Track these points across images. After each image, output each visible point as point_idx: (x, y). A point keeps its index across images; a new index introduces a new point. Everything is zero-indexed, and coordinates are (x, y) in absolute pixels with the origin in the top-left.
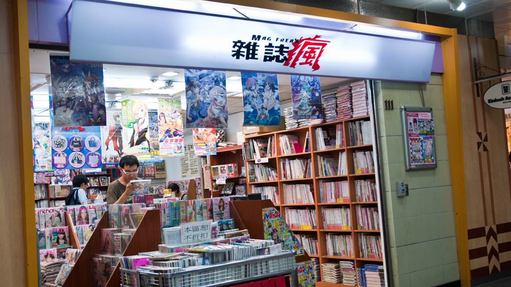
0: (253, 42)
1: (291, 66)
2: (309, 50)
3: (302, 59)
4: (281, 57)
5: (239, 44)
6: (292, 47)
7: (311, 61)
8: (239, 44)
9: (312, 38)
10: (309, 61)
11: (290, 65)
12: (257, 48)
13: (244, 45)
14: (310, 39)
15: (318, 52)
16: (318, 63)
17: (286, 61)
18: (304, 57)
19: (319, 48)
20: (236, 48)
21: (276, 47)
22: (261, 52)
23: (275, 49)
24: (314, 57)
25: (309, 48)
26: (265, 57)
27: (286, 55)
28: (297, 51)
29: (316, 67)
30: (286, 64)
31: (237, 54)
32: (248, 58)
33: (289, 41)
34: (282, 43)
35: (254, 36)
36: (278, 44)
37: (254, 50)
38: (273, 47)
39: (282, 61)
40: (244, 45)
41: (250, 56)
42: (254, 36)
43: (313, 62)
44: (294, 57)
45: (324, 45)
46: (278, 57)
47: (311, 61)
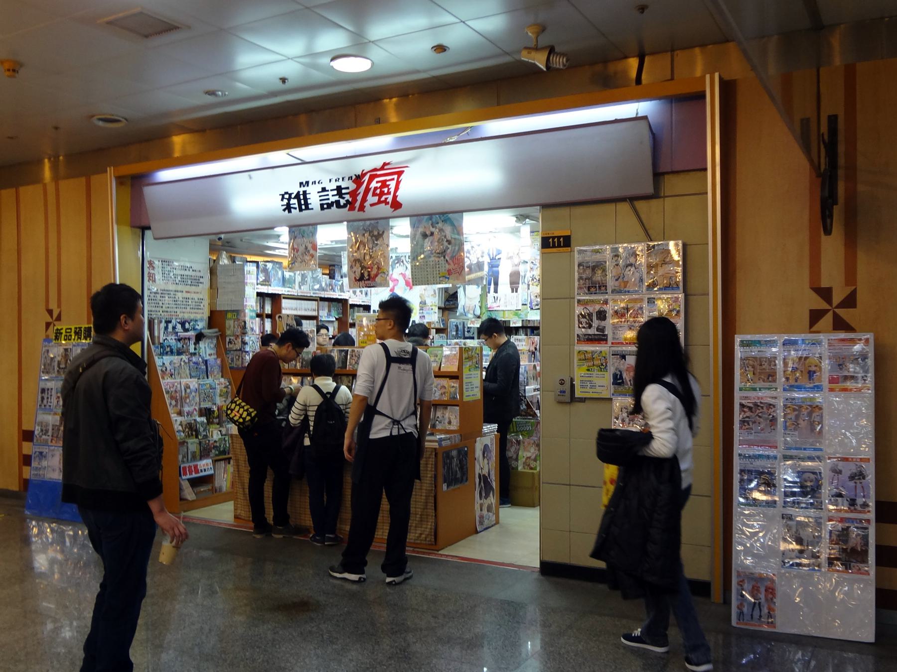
0: (302, 190)
1: (359, 210)
3: (371, 199)
4: (342, 202)
6: (353, 186)
7: (386, 199)
10: (383, 199)
13: (293, 196)
14: (375, 170)
15: (392, 185)
16: (398, 199)
17: (350, 205)
18: (374, 194)
19: (393, 179)
20: (285, 201)
22: (314, 200)
23: (331, 193)
24: (389, 193)
25: (377, 182)
26: (322, 205)
27: (347, 197)
30: (352, 208)
31: (288, 208)
32: (301, 210)
34: (338, 184)
35: (301, 184)
37: (306, 199)
39: (345, 206)
40: (293, 196)
41: (303, 207)
42: (301, 184)
43: (390, 198)
44: (359, 198)
45: (400, 174)
46: (337, 202)
47: (386, 199)
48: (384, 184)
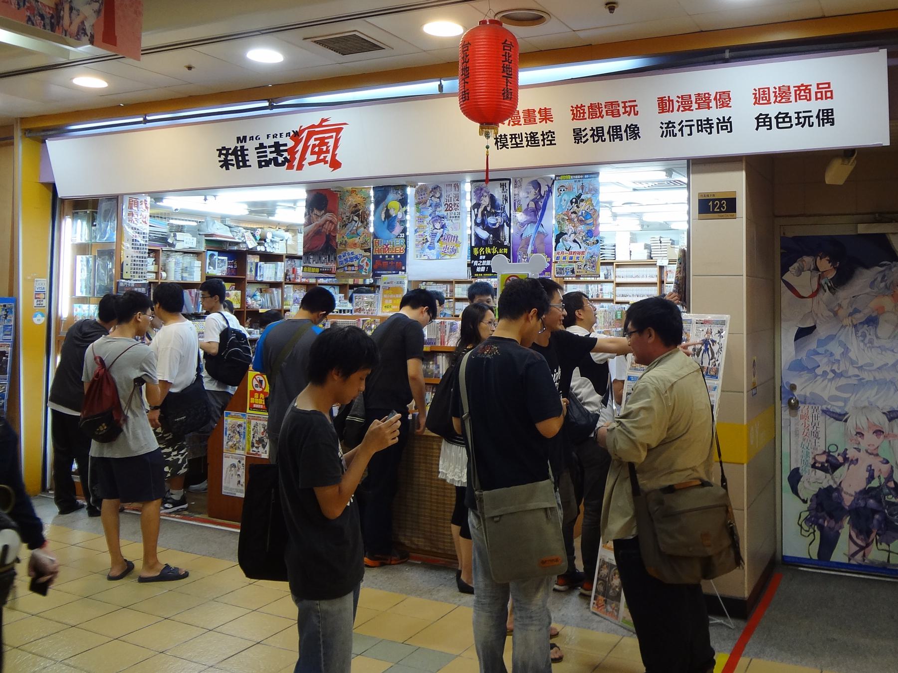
2: (317, 142)
3: (310, 158)
4: (280, 159)
5: (224, 152)
6: (291, 143)
7: (325, 157)
8: (224, 152)
9: (316, 124)
10: (322, 157)
11: (295, 167)
12: (246, 152)
14: (313, 126)
17: (288, 162)
18: (313, 153)
19: (331, 137)
20: (223, 157)
21: (270, 147)
22: (252, 157)
23: (269, 150)
24: (327, 151)
25: (316, 139)
26: (260, 162)
27: (286, 154)
28: (300, 147)
29: (335, 164)
30: (290, 167)
33: (284, 135)
34: (276, 140)
35: (238, 138)
36: (271, 141)
37: (244, 156)
38: (265, 147)
39: (283, 164)
41: (241, 164)
42: (238, 138)
43: (329, 158)
44: (298, 156)
45: (338, 131)
46: (275, 159)
47: (325, 157)
48: (323, 142)
